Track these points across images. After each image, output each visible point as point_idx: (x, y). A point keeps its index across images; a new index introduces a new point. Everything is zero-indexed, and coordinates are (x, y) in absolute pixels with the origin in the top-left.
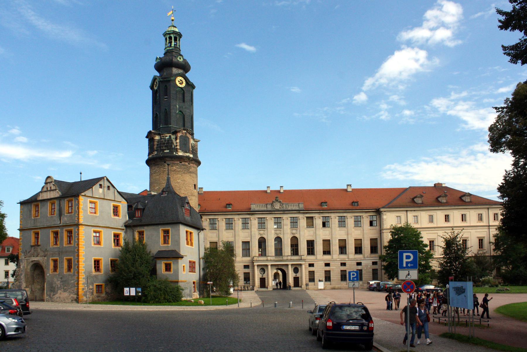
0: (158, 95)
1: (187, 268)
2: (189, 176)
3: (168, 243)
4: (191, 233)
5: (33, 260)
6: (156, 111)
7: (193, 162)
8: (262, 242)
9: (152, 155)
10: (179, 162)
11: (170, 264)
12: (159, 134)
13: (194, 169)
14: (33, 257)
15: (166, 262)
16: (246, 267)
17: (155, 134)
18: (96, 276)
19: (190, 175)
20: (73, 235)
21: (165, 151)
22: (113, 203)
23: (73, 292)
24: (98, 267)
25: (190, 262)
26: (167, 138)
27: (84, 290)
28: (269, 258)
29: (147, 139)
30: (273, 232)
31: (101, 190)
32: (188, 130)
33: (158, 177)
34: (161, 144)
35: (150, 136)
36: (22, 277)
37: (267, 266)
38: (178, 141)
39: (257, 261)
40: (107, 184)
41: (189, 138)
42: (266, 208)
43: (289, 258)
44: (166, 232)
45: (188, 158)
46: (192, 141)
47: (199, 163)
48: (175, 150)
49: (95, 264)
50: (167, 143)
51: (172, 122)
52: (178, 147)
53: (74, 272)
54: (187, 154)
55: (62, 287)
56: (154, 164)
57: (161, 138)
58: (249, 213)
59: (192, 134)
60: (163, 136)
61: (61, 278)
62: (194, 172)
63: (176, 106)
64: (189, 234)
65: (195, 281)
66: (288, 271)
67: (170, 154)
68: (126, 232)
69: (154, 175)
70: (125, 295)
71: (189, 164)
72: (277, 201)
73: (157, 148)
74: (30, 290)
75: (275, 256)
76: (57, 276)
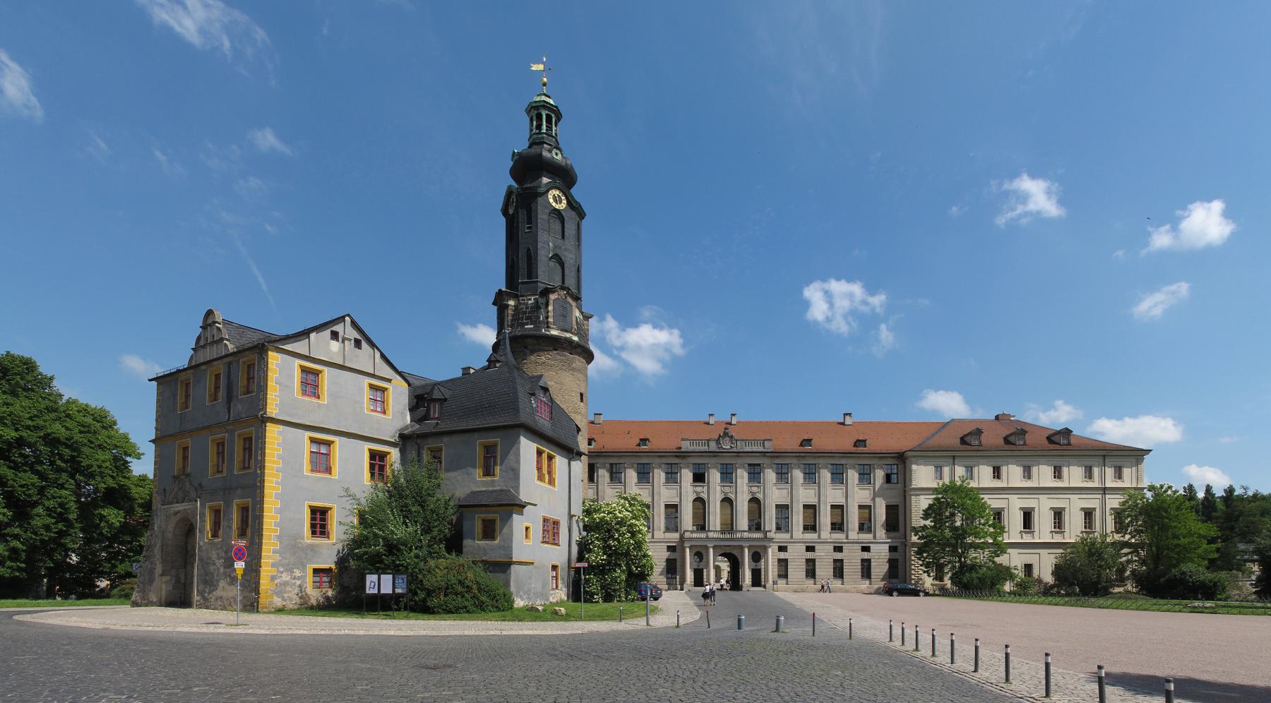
1: (537, 530)
3: (494, 475)
21: (526, 327)
23: (247, 584)
24: (323, 527)
26: (530, 302)
27: (277, 581)
29: (496, 307)
31: (335, 346)
32: (569, 289)
35: (499, 300)
36: (157, 550)
40: (353, 334)
48: (544, 324)
49: (313, 519)
50: (530, 312)
51: (540, 272)
59: (577, 299)
60: (523, 300)
63: (547, 243)
68: (402, 452)
70: (368, 592)
74: (174, 581)
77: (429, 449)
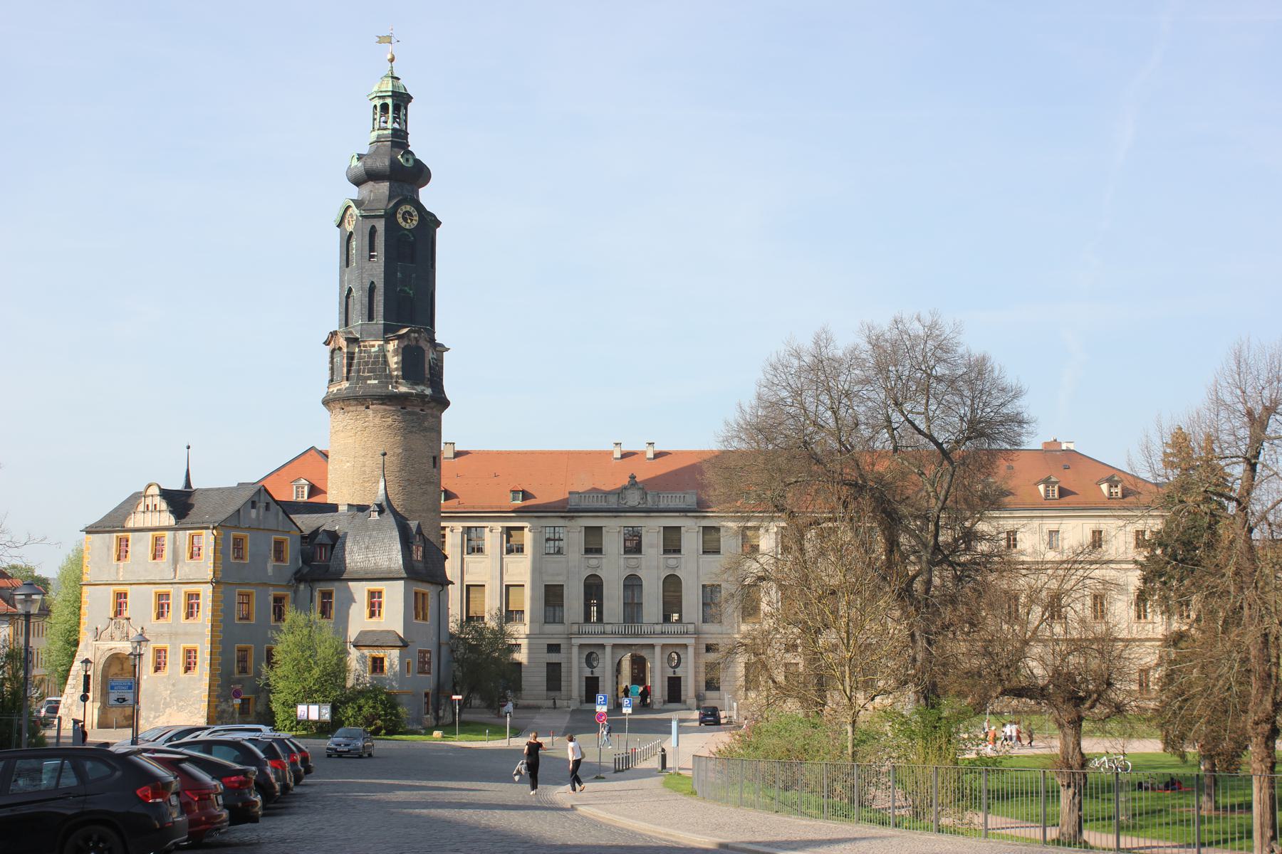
0: (354, 243)
2: (422, 438)
5: (113, 646)
6: (349, 282)
7: (432, 404)
8: (593, 588)
9: (339, 387)
10: (399, 407)
13: (434, 420)
14: (112, 639)
18: (239, 681)
19: (424, 437)
20: (201, 601)
21: (369, 382)
22: (274, 537)
26: (373, 350)
34: (359, 363)
37: (602, 646)
41: (424, 350)
42: (603, 503)
43: (658, 628)
45: (422, 396)
46: (430, 355)
50: (374, 363)
53: (201, 674)
54: (419, 388)
55: (175, 702)
56: (343, 409)
57: (360, 352)
58: (563, 514)
61: (174, 685)
62: (433, 429)
65: (428, 690)
67: (379, 390)
69: (342, 434)
71: (422, 410)
73: (349, 372)
76: (165, 680)
77: (320, 591)
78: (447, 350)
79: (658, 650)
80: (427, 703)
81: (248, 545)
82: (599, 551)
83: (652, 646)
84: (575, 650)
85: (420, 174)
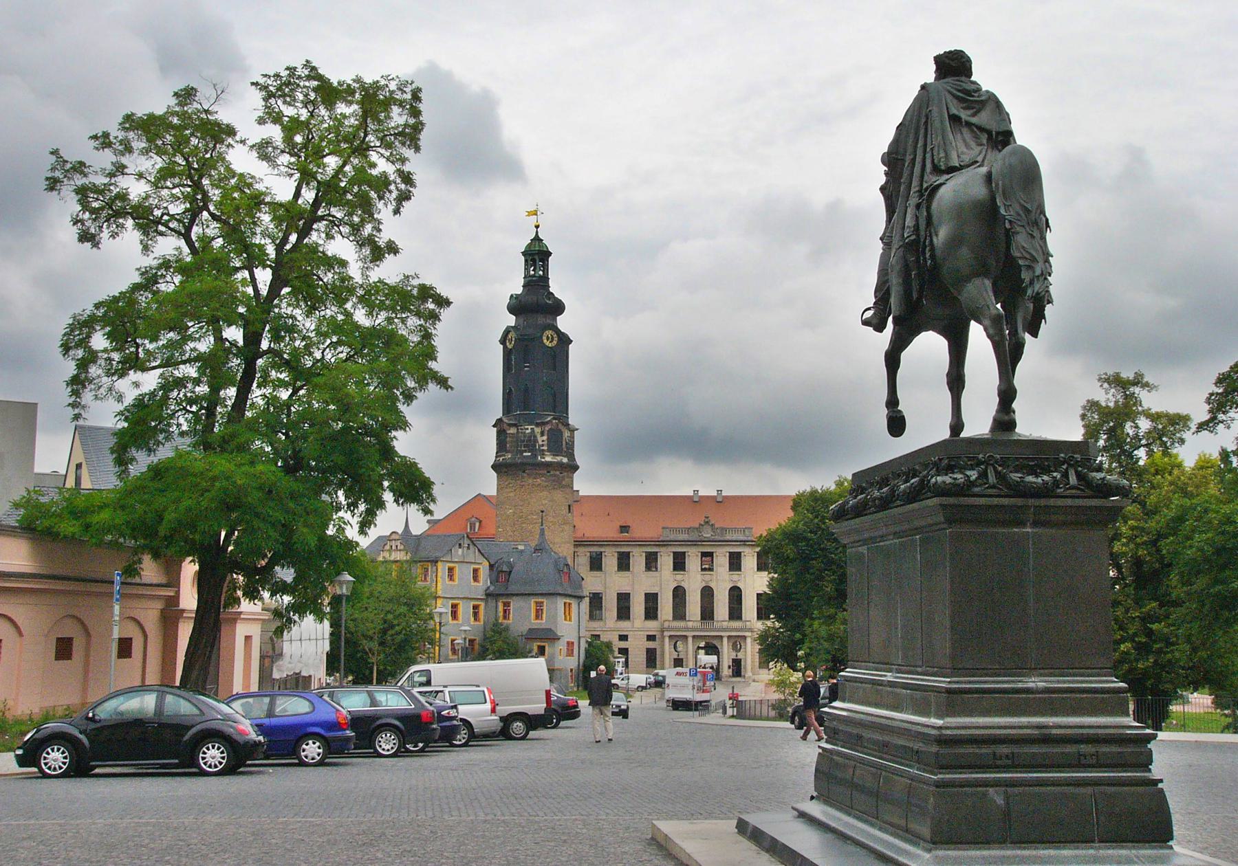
3: (542, 619)
4: (570, 604)
8: (679, 594)
11: (544, 647)
12: (515, 425)
15: (539, 644)
16: (651, 638)
17: (510, 425)
21: (524, 454)
25: (568, 643)
26: (527, 431)
28: (690, 624)
30: (699, 577)
33: (512, 494)
38: (545, 438)
39: (669, 629)
43: (725, 624)
44: (539, 604)
45: (560, 465)
46: (566, 434)
47: (576, 468)
52: (545, 448)
54: (559, 458)
57: (518, 432)
64: (567, 605)
66: (722, 648)
72: (707, 523)
75: (702, 619)
78: (577, 429)
79: (725, 640)
80: (572, 676)
81: (457, 571)
82: (683, 569)
83: (721, 637)
84: (667, 640)
85: (558, 308)
